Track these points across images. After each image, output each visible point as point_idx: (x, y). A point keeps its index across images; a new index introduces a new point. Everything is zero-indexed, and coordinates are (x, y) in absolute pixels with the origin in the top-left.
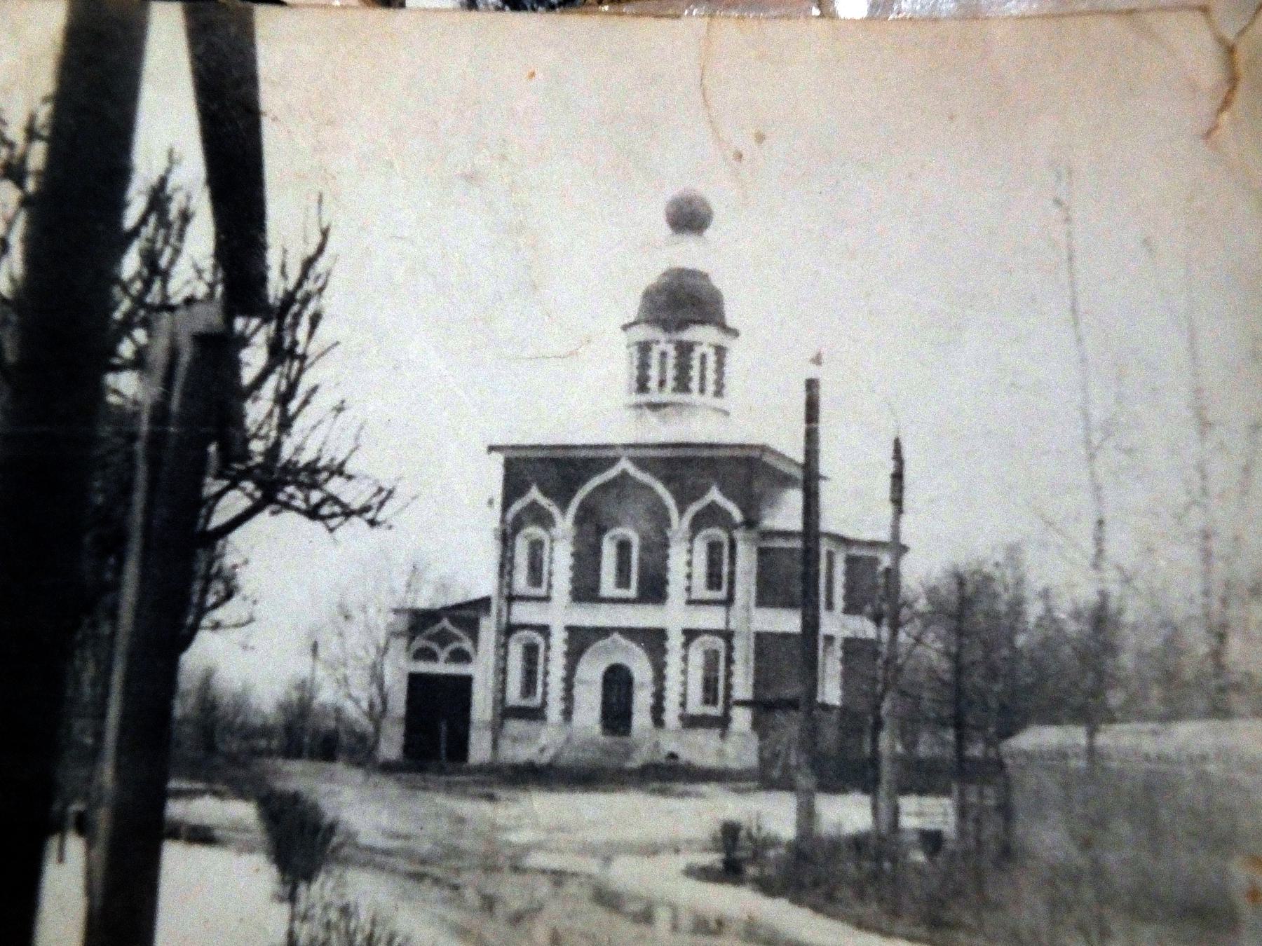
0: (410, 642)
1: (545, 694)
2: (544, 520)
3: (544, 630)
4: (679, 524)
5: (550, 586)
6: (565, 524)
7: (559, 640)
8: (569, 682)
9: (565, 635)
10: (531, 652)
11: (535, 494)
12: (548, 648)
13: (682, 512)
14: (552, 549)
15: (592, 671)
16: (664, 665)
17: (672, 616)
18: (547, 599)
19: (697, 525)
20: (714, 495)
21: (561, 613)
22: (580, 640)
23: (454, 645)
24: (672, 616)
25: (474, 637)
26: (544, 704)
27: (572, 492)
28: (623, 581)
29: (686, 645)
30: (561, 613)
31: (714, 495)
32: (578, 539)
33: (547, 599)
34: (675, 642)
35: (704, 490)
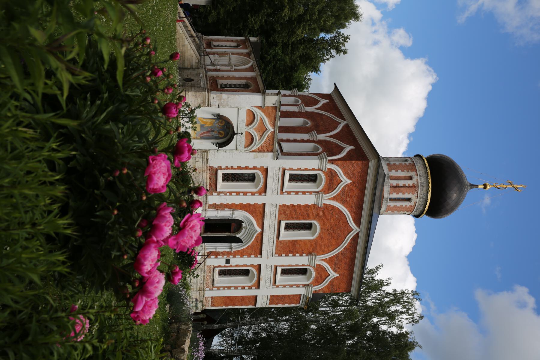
0: (259, 108)
1: (225, 194)
2: (329, 188)
3: (264, 190)
4: (320, 260)
5: (289, 193)
6: (327, 200)
7: (258, 200)
8: (232, 207)
9: (260, 203)
10: (251, 178)
11: (346, 181)
12: (253, 194)
13: (324, 260)
14: (311, 193)
15: (239, 215)
16: (242, 257)
17: (269, 260)
18: (282, 193)
21: (272, 201)
22: (259, 212)
23: (256, 135)
24: (269, 260)
25: (260, 150)
26: (219, 194)
27: (343, 203)
29: (252, 266)
30: (272, 201)
31: (333, 275)
32: (314, 206)
33: (282, 193)
34: (253, 261)
35: (335, 270)
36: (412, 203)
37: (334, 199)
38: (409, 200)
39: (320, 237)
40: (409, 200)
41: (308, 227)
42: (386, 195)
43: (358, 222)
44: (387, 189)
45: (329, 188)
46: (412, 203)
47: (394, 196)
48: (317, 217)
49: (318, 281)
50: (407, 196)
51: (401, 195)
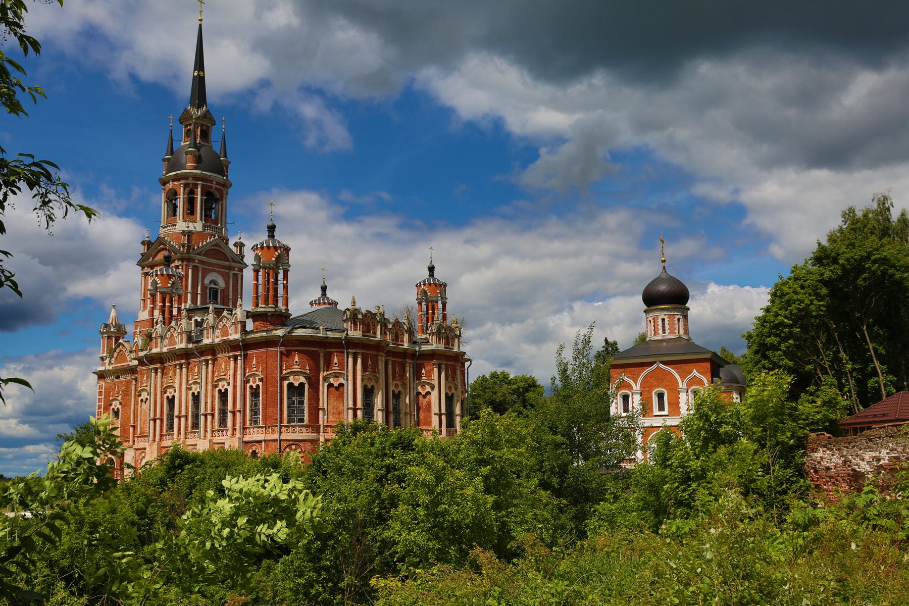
4: (682, 385)
6: (636, 387)
19: (689, 385)
20: (695, 373)
28: (661, 408)
36: (666, 318)
37: (636, 383)
38: (663, 320)
39: (664, 387)
40: (663, 320)
41: (661, 396)
42: (659, 338)
43: (654, 363)
44: (656, 338)
45: (629, 387)
46: (666, 318)
47: (660, 331)
48: (650, 392)
49: (701, 383)
50: (660, 323)
51: (660, 327)
